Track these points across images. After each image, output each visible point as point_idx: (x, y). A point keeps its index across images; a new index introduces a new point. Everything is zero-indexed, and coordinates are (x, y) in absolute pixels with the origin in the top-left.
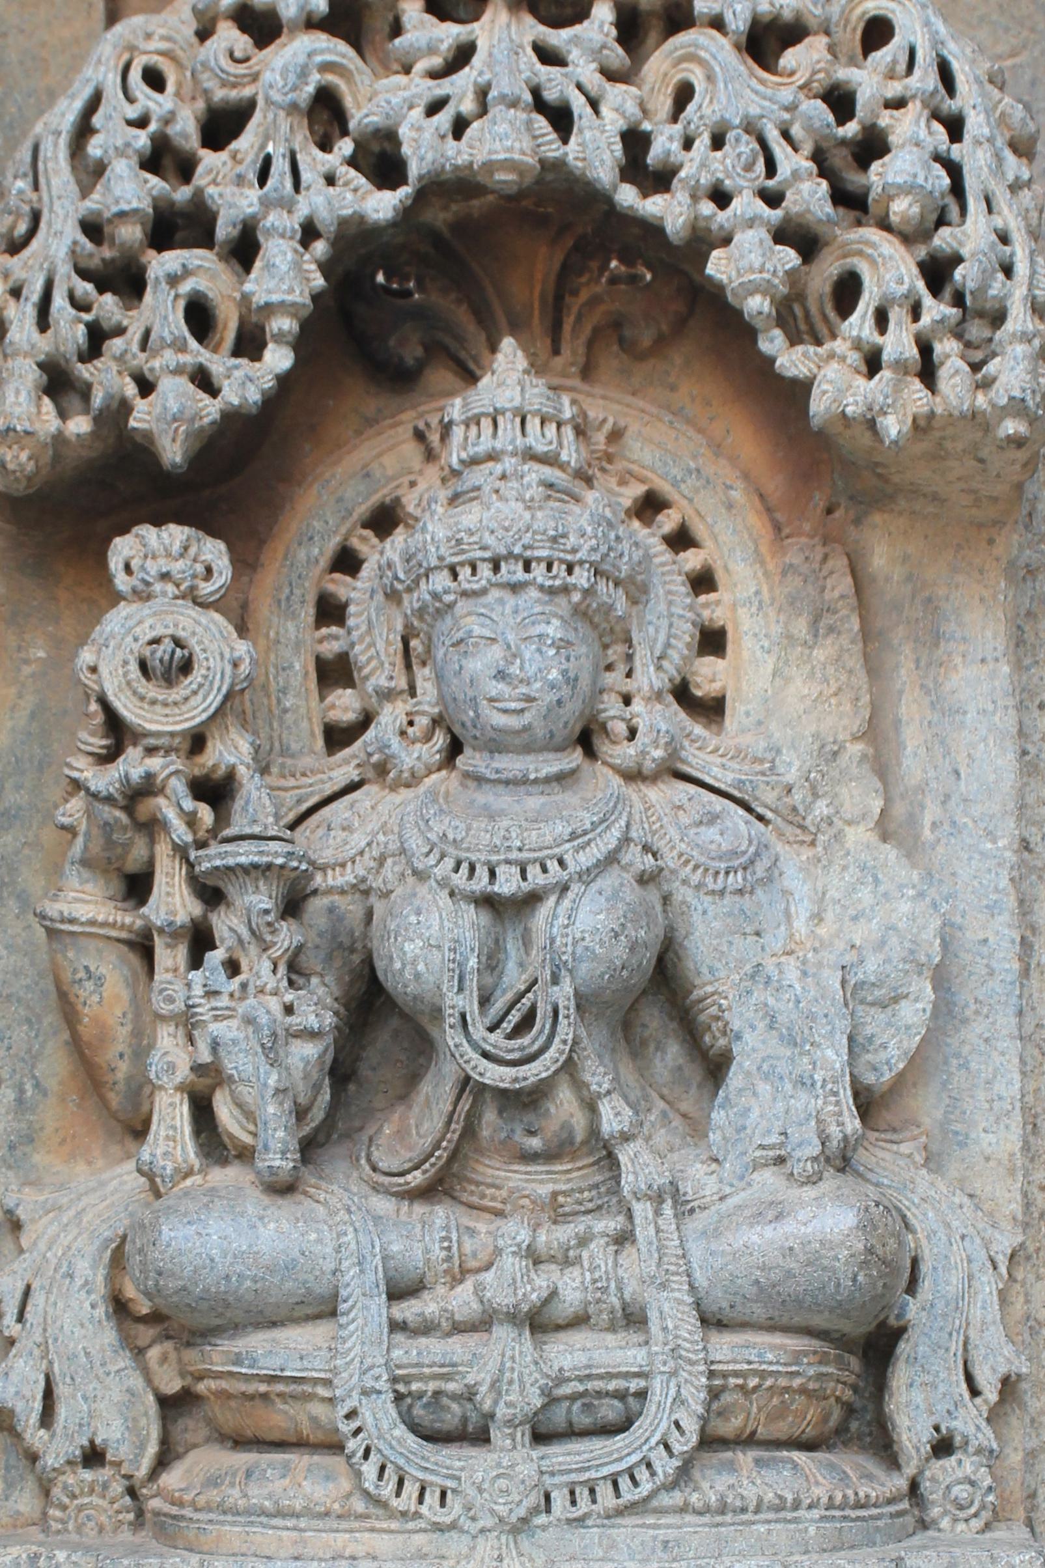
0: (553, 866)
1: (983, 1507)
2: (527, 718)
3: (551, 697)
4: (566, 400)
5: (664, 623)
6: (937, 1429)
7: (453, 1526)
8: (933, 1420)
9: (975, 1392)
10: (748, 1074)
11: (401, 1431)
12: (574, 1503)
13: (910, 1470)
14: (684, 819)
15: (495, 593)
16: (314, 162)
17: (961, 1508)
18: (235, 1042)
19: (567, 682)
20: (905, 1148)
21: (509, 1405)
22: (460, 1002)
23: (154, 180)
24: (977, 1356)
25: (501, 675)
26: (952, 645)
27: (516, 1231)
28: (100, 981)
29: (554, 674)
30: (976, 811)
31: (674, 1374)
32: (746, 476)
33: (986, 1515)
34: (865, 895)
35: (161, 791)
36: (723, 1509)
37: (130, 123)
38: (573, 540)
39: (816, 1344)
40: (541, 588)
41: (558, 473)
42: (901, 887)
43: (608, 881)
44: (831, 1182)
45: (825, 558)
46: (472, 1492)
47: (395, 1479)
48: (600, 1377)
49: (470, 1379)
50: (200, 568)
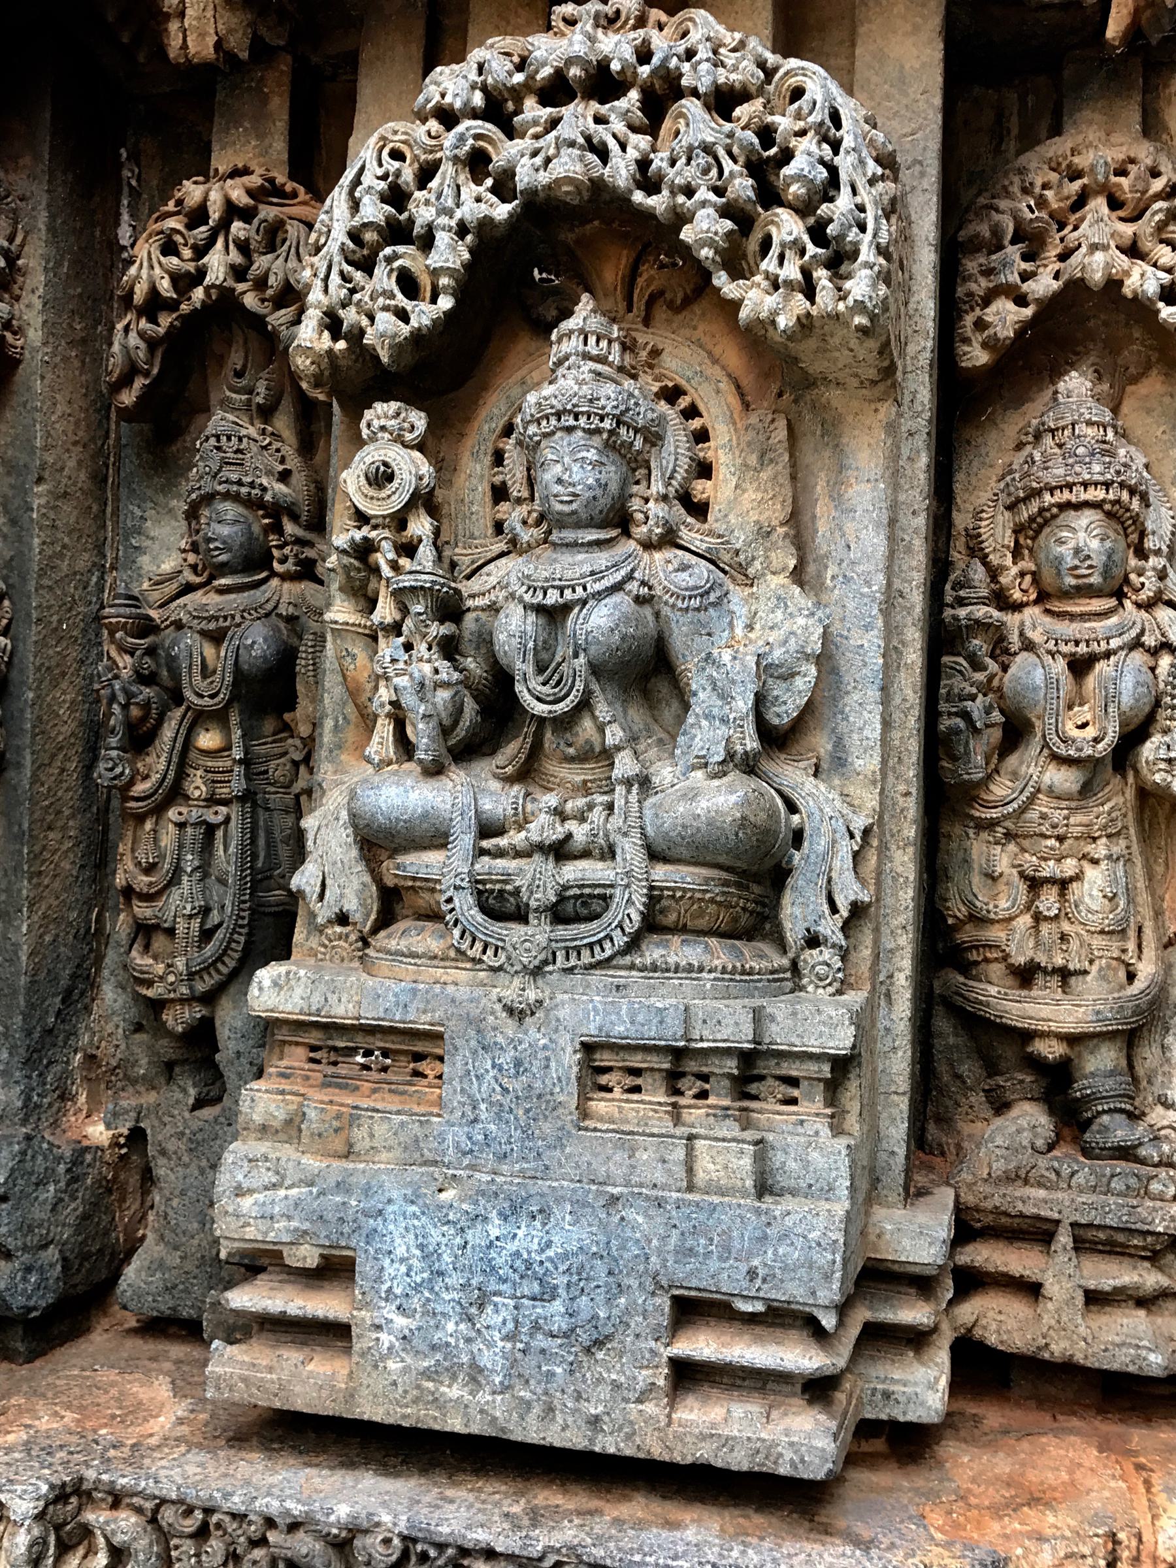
0: (579, 590)
1: (835, 980)
2: (574, 506)
3: (589, 494)
4: (615, 327)
5: (672, 458)
6: (808, 930)
7: (500, 968)
8: (806, 925)
9: (834, 910)
10: (697, 715)
11: (475, 911)
12: (568, 959)
13: (791, 955)
14: (670, 568)
15: (559, 434)
16: (470, 190)
17: (821, 980)
18: (405, 688)
19: (600, 485)
20: (802, 765)
21: (537, 900)
22: (524, 667)
23: (387, 208)
24: (836, 889)
25: (559, 481)
26: (850, 472)
27: (551, 799)
28: (354, 657)
29: (591, 481)
30: (860, 569)
31: (627, 886)
32: (729, 375)
33: (836, 985)
34: (779, 615)
35: (377, 550)
36: (655, 968)
37: (378, 178)
38: (603, 402)
39: (724, 875)
40: (584, 430)
41: (607, 368)
42: (800, 609)
43: (617, 598)
44: (734, 776)
45: (773, 421)
46: (511, 949)
47: (470, 939)
48: (589, 886)
49: (517, 884)
50: (406, 425)
